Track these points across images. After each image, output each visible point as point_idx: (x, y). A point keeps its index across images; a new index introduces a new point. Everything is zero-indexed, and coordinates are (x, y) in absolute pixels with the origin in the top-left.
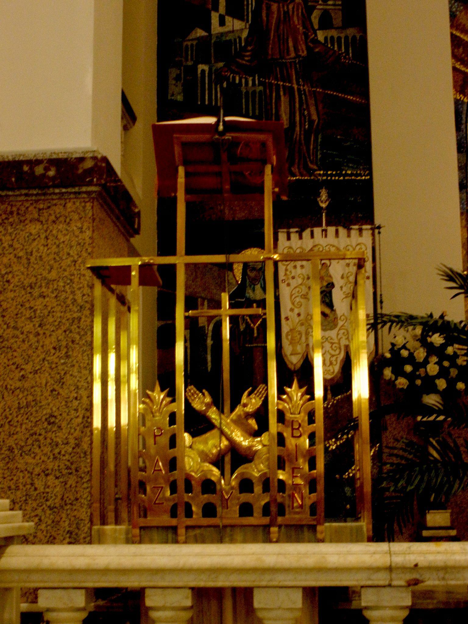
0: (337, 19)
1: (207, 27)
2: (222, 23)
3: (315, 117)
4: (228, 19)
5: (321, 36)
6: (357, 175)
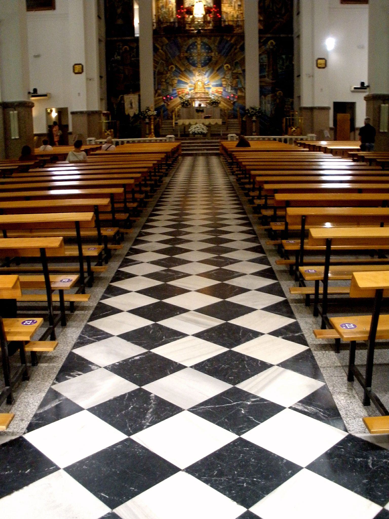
1: (114, 58)
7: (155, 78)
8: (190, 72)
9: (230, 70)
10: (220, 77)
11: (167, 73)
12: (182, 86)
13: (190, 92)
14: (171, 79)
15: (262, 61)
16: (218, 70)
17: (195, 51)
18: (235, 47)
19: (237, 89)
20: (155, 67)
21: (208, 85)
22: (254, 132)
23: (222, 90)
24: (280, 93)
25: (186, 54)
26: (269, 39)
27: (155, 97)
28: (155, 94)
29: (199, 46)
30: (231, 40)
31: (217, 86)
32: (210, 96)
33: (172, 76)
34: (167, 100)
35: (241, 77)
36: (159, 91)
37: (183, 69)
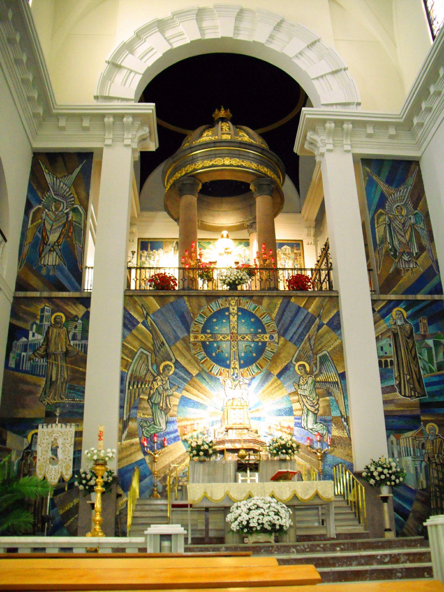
0: (79, 336)
1: (27, 337)
2: (33, 335)
3: (66, 376)
4: (36, 334)
5: (72, 343)
6: (80, 401)
7: (122, 391)
8: (213, 378)
9: (311, 373)
10: (285, 391)
11: (155, 380)
12: (191, 412)
13: (211, 430)
14: (165, 394)
15: (382, 354)
16: (280, 375)
17: (225, 330)
18: (317, 321)
19: (331, 421)
20: (126, 365)
21: (258, 410)
22: (389, 530)
23: (292, 425)
24: (433, 429)
25: (202, 337)
26: (393, 304)
27: (120, 439)
28: (122, 431)
29: (234, 319)
30: (306, 307)
31: (280, 413)
32: (262, 439)
33: (168, 386)
34: (152, 448)
35: (337, 393)
36: (133, 425)
37: (194, 372)
